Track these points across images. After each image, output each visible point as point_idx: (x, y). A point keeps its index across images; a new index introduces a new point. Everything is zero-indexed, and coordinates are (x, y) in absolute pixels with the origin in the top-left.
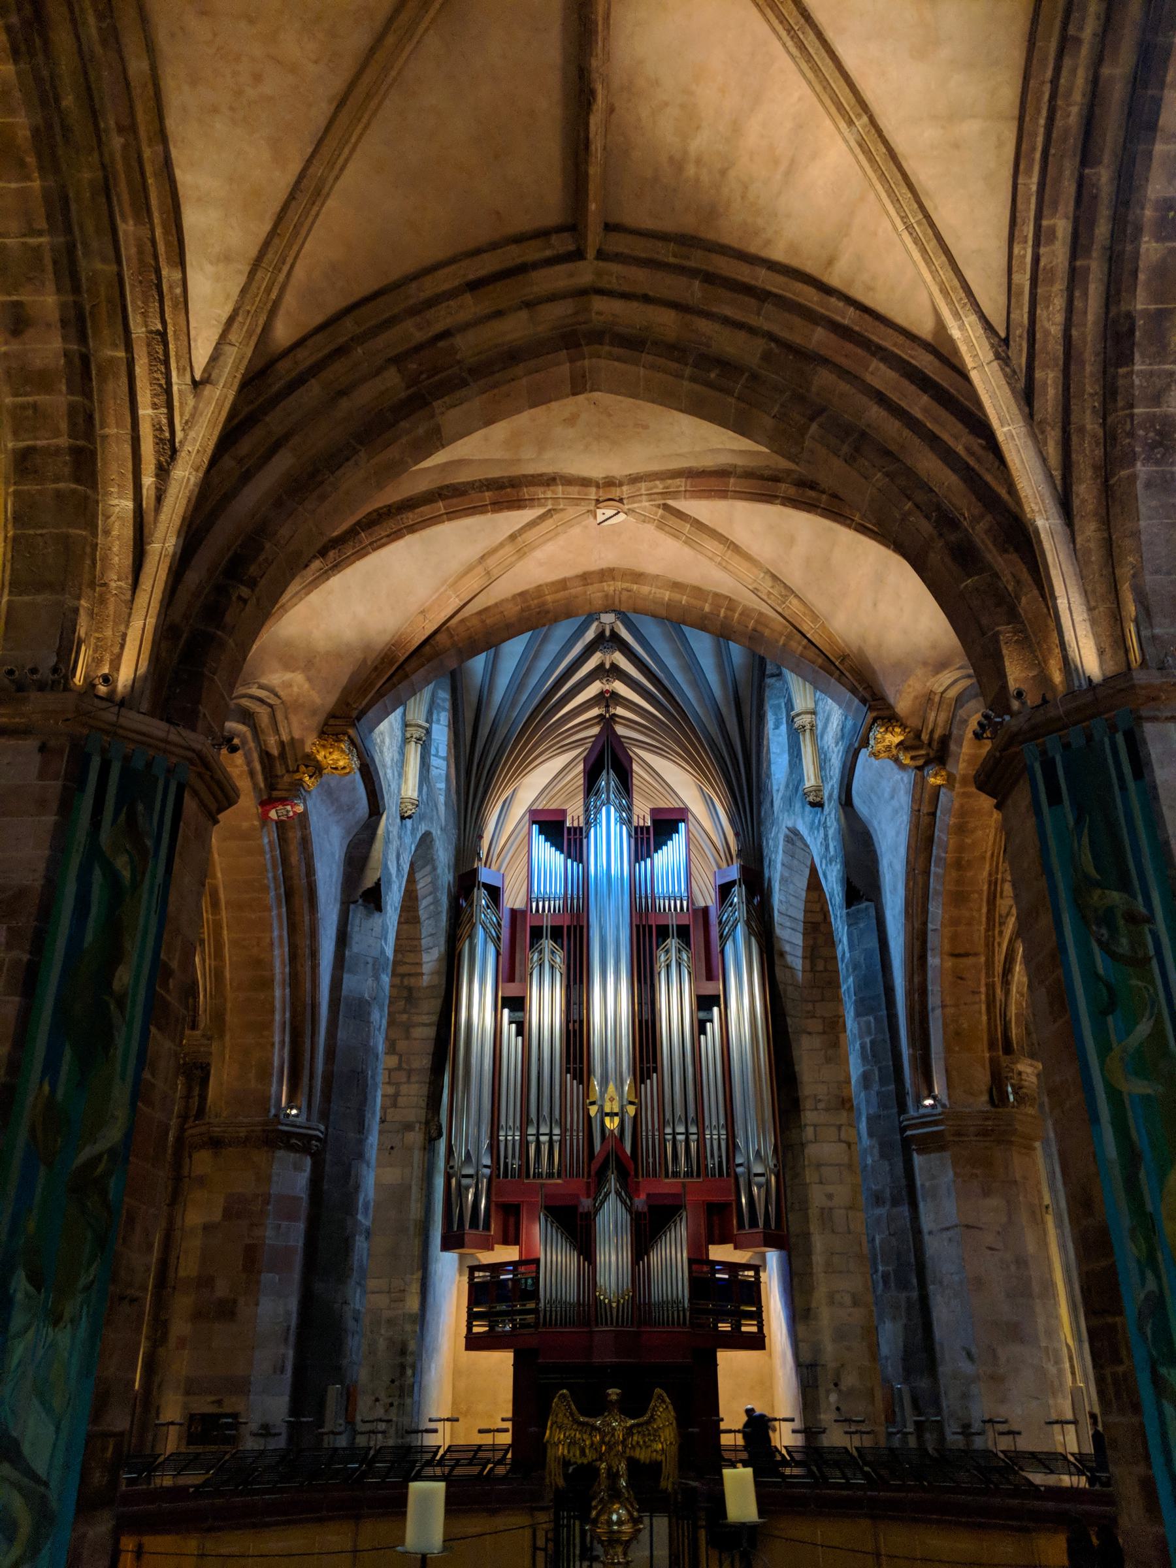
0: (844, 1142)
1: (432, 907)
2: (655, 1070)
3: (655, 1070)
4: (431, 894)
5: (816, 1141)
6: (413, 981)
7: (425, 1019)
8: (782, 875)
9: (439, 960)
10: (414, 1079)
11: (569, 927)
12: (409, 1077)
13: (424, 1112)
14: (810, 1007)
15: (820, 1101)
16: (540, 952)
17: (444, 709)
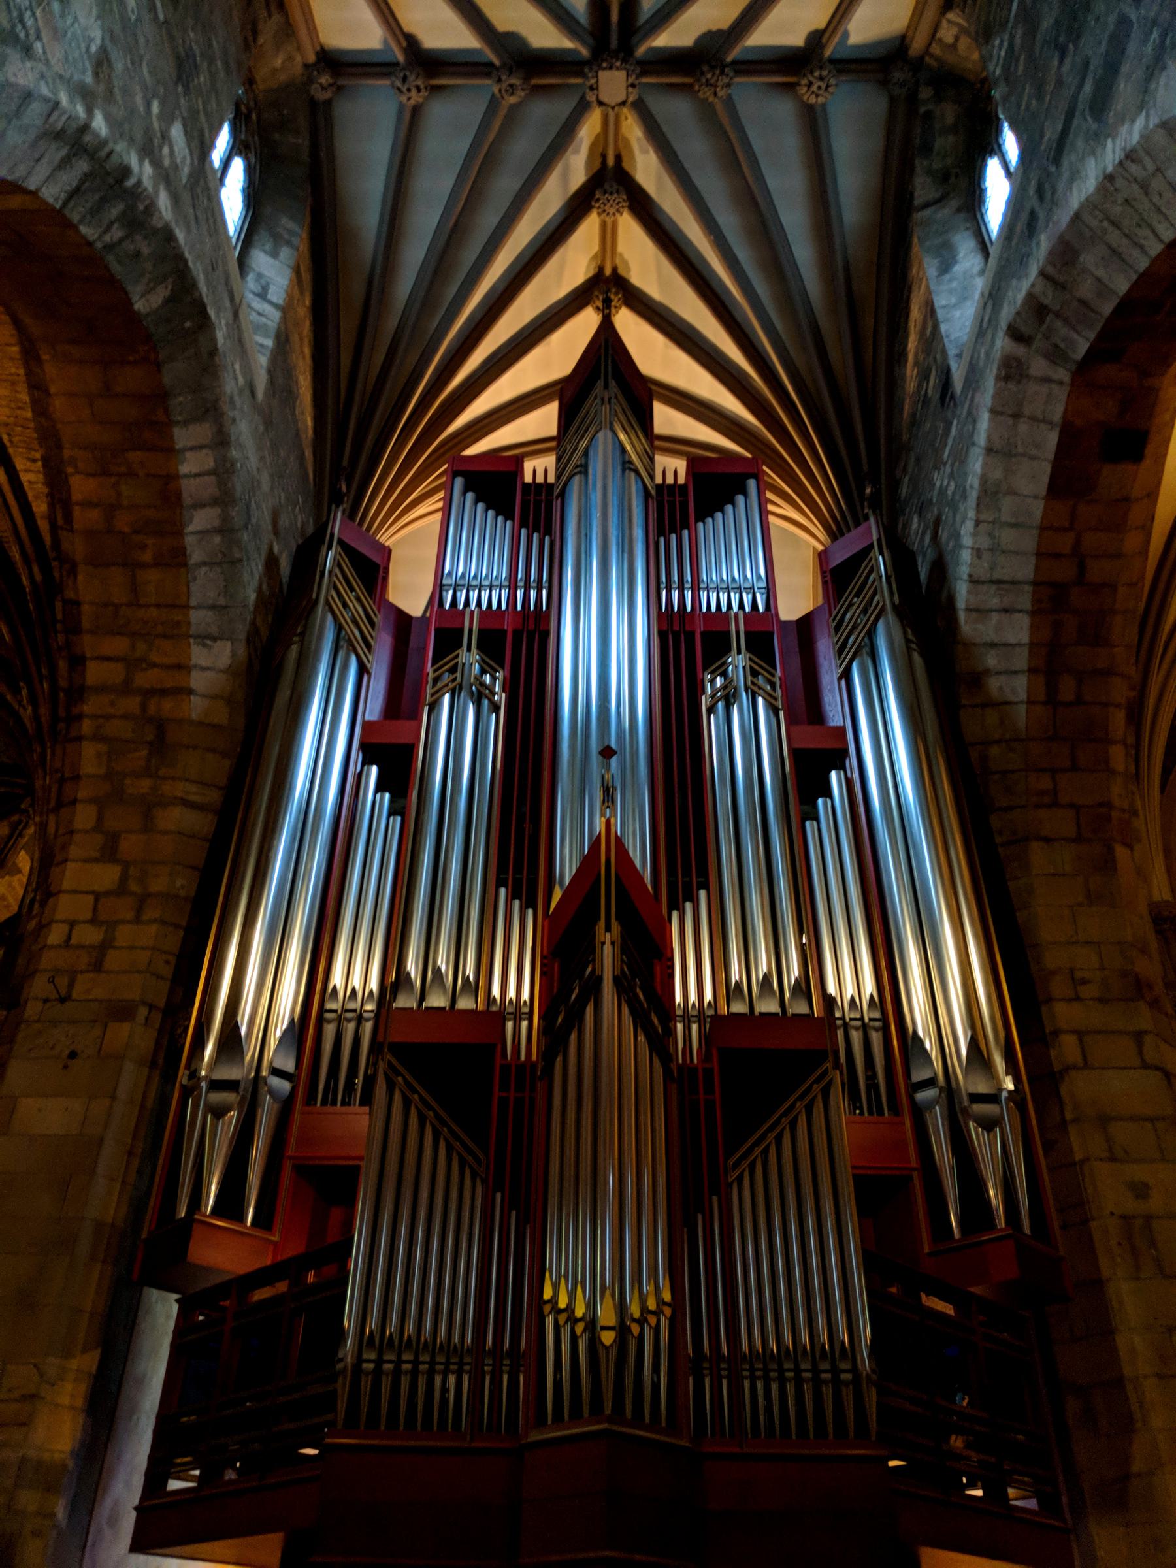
0: (1157, 1068)
1: (217, 539)
2: (705, 886)
3: (705, 886)
4: (215, 502)
5: (1086, 1065)
6: (167, 706)
7: (194, 793)
8: (984, 479)
9: (231, 671)
10: (148, 914)
11: (517, 634)
12: (139, 911)
13: (165, 987)
14: (1045, 783)
15: (1084, 982)
16: (453, 670)
17: (289, 243)
